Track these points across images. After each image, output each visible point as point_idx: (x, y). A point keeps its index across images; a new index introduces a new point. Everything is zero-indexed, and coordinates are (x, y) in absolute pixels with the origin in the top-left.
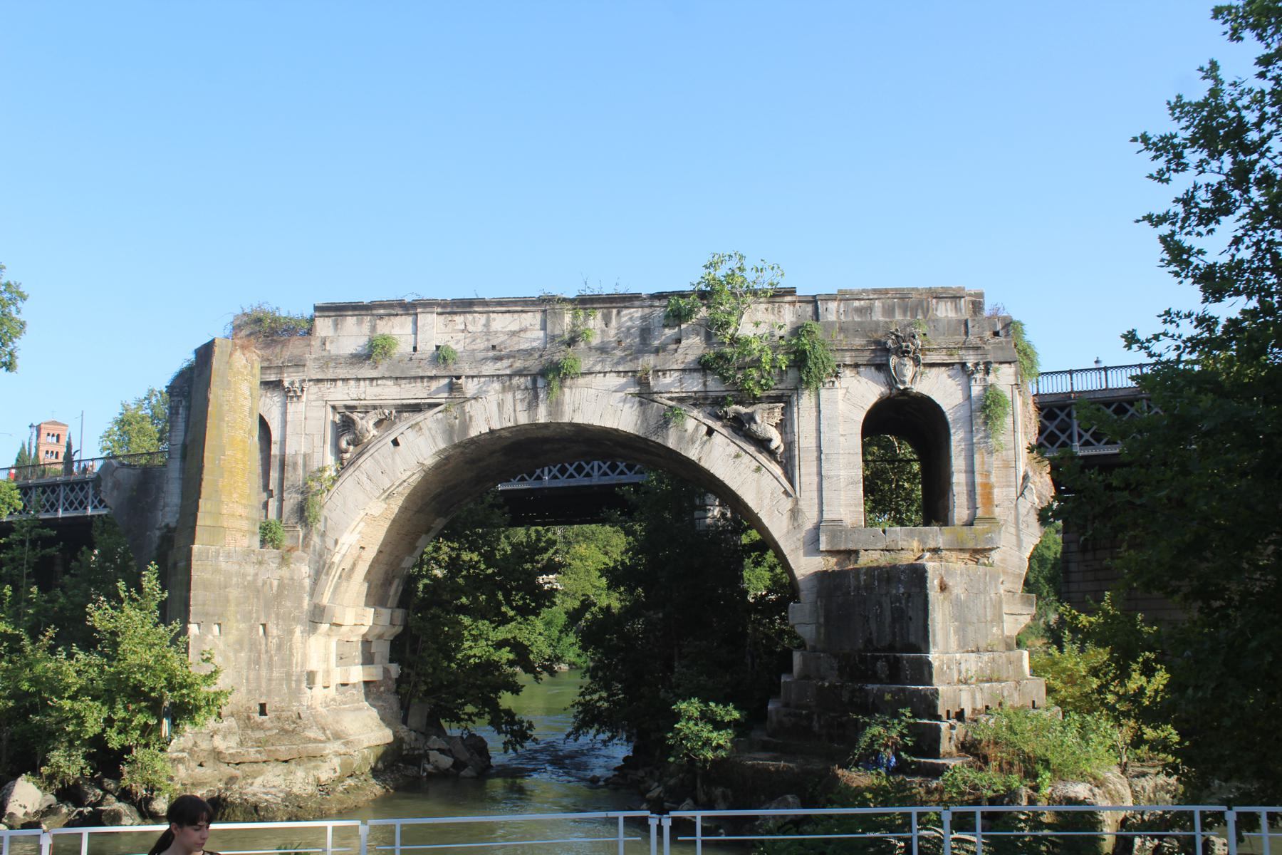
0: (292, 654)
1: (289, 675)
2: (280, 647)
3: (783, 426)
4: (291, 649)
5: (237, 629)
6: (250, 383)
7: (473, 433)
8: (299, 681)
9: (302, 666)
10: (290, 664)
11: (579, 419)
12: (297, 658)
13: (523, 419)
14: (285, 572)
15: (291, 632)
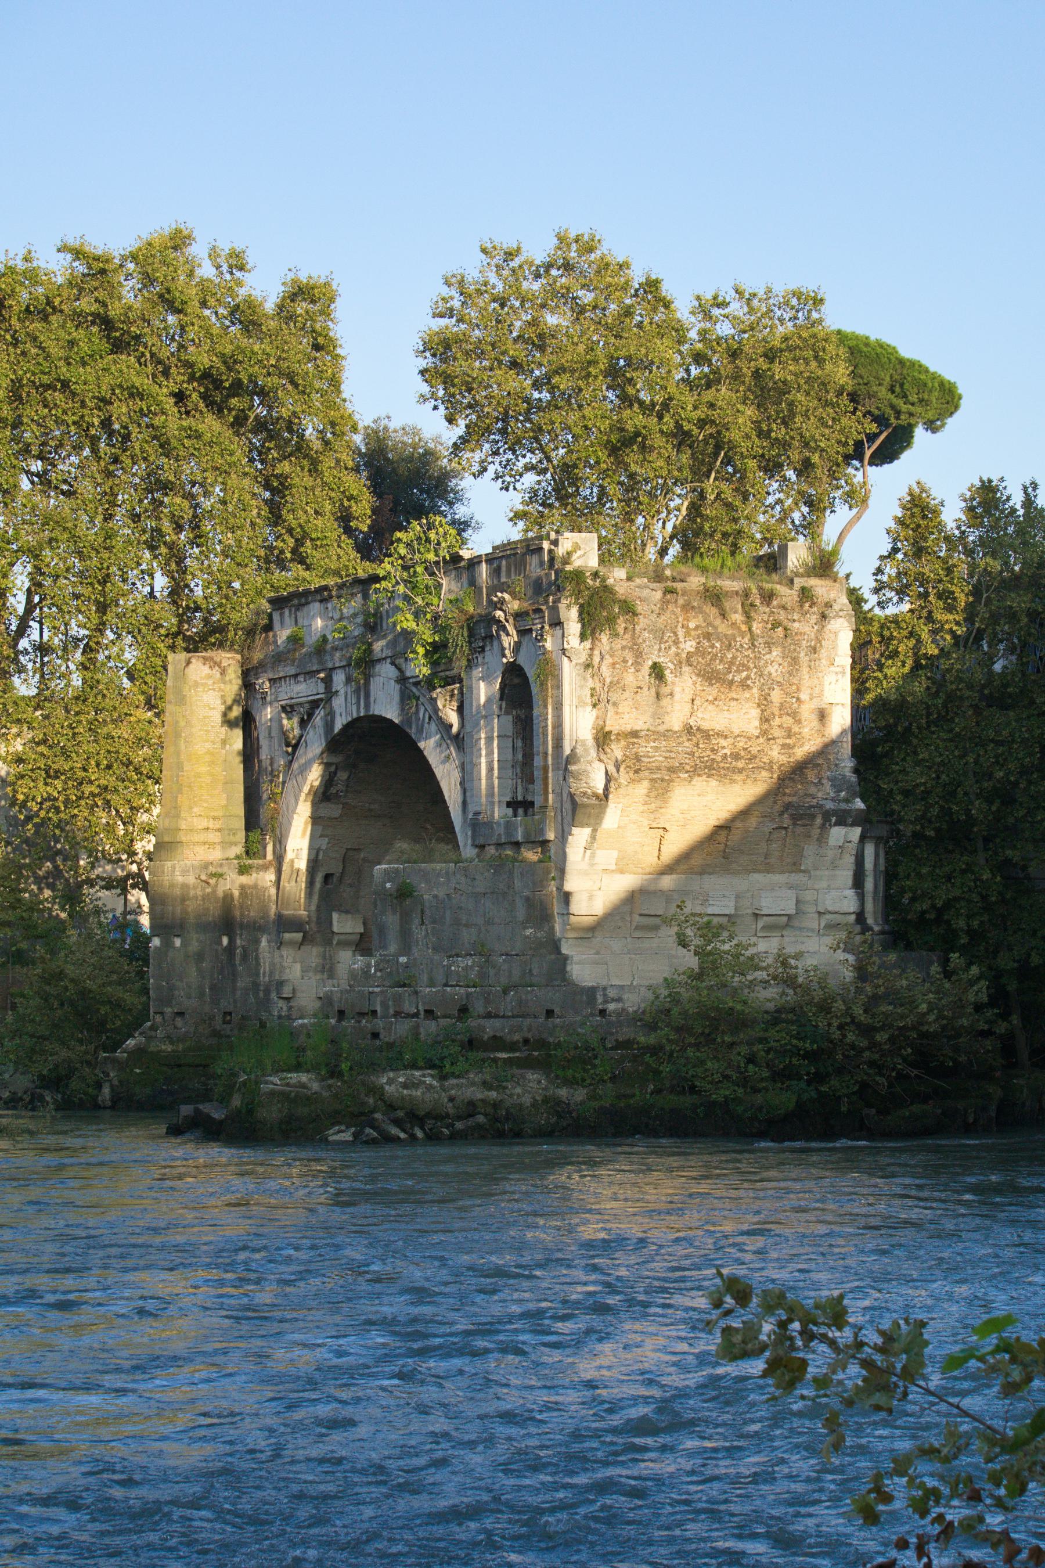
0: (258, 964)
1: (256, 985)
2: (245, 957)
3: (460, 710)
4: (257, 958)
5: (198, 940)
6: (220, 690)
7: (336, 731)
8: (267, 991)
9: (270, 976)
10: (258, 975)
11: (377, 713)
12: (265, 967)
13: (355, 715)
14: (244, 879)
15: (258, 942)
